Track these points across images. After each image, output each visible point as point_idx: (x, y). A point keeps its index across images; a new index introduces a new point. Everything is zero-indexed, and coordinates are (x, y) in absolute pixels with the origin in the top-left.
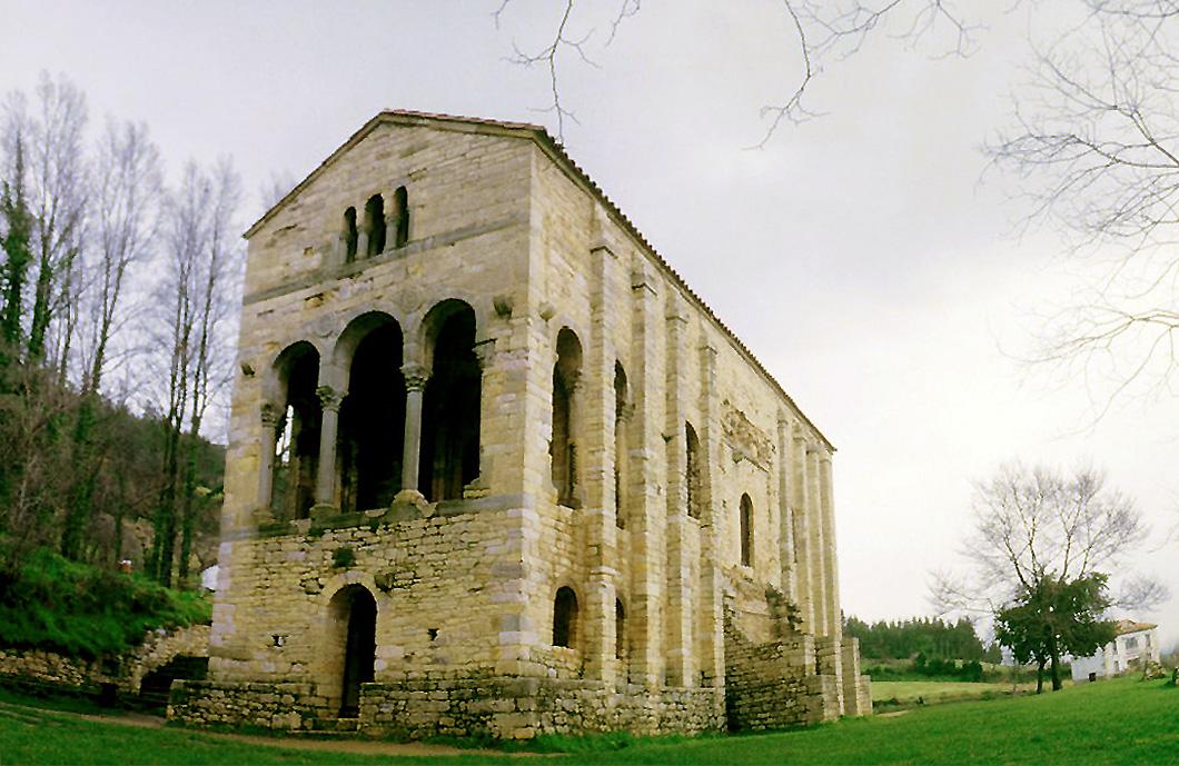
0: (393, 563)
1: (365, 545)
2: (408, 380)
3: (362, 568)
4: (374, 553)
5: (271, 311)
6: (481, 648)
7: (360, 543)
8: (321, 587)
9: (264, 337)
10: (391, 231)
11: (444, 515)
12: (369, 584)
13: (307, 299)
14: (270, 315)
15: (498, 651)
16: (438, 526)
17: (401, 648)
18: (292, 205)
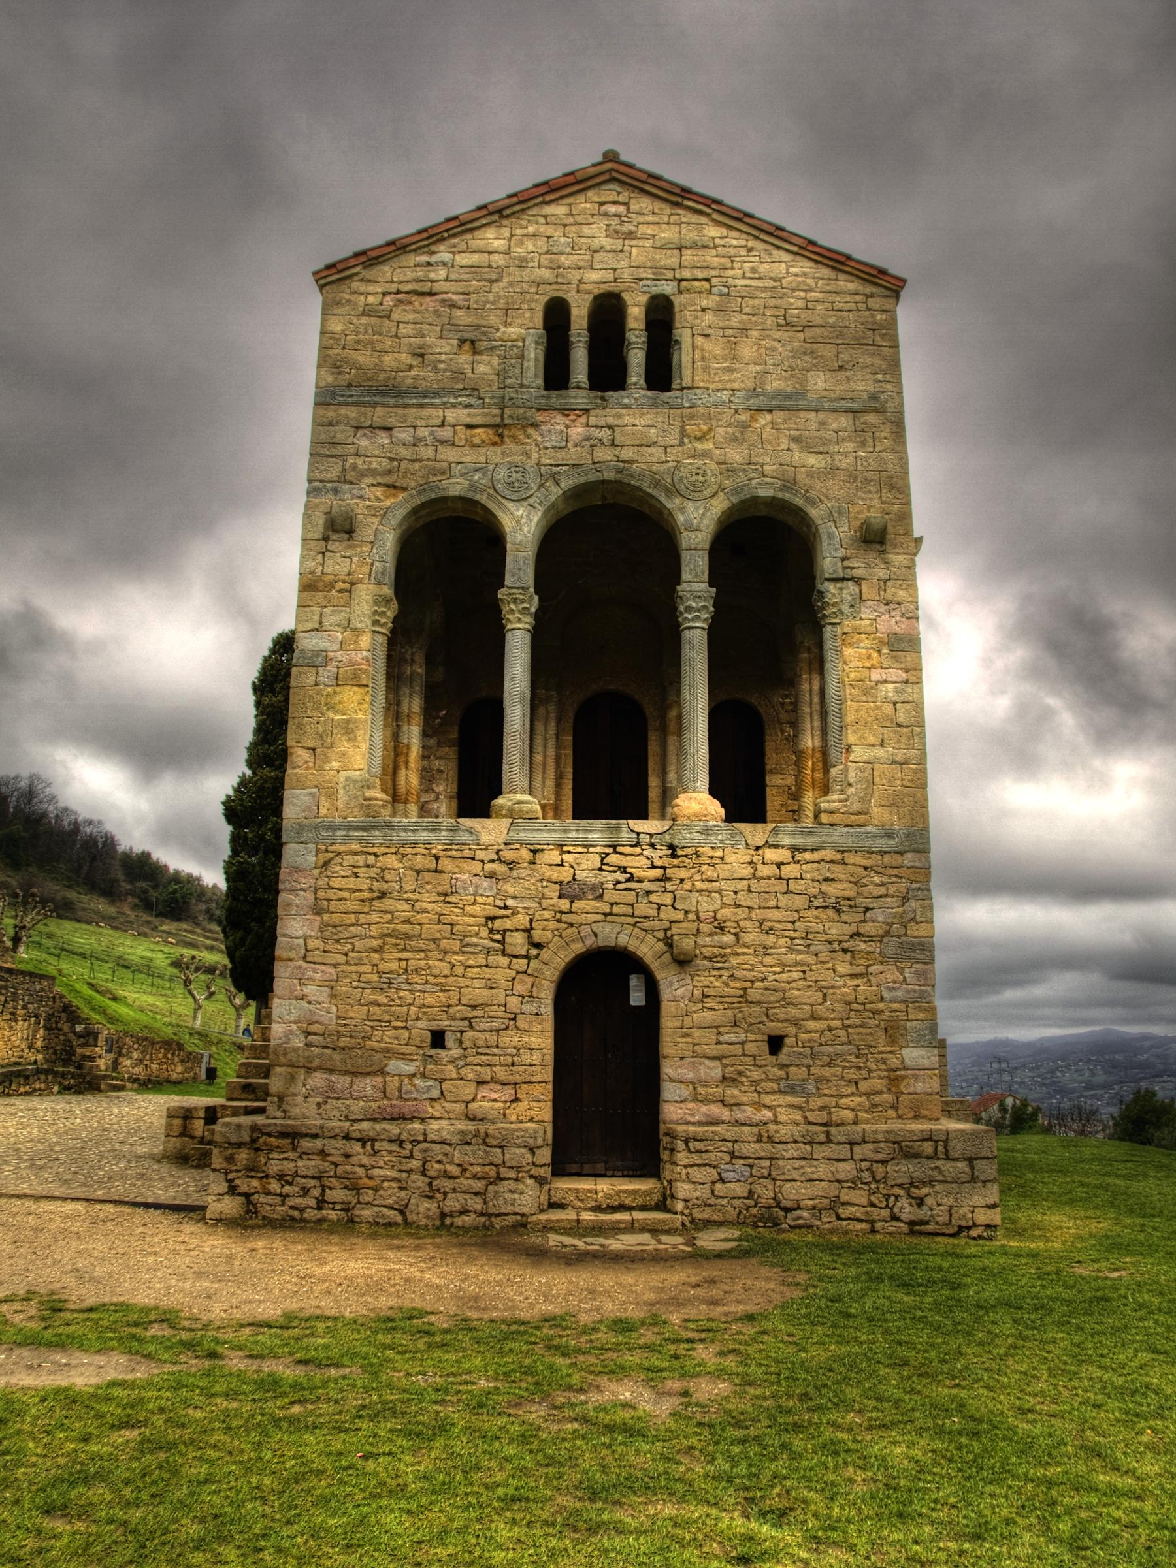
0: (691, 916)
1: (628, 880)
2: (689, 609)
3: (631, 920)
4: (653, 898)
5: (390, 429)
6: (870, 1071)
7: (619, 876)
8: (538, 946)
9: (373, 473)
10: (636, 359)
11: (795, 849)
12: (647, 949)
13: (470, 427)
14: (383, 434)
15: (904, 1077)
16: (779, 865)
17: (717, 1063)
18: (424, 258)
